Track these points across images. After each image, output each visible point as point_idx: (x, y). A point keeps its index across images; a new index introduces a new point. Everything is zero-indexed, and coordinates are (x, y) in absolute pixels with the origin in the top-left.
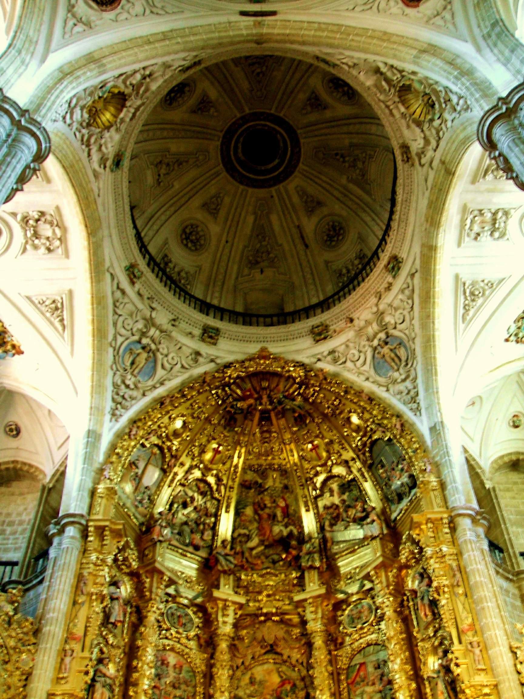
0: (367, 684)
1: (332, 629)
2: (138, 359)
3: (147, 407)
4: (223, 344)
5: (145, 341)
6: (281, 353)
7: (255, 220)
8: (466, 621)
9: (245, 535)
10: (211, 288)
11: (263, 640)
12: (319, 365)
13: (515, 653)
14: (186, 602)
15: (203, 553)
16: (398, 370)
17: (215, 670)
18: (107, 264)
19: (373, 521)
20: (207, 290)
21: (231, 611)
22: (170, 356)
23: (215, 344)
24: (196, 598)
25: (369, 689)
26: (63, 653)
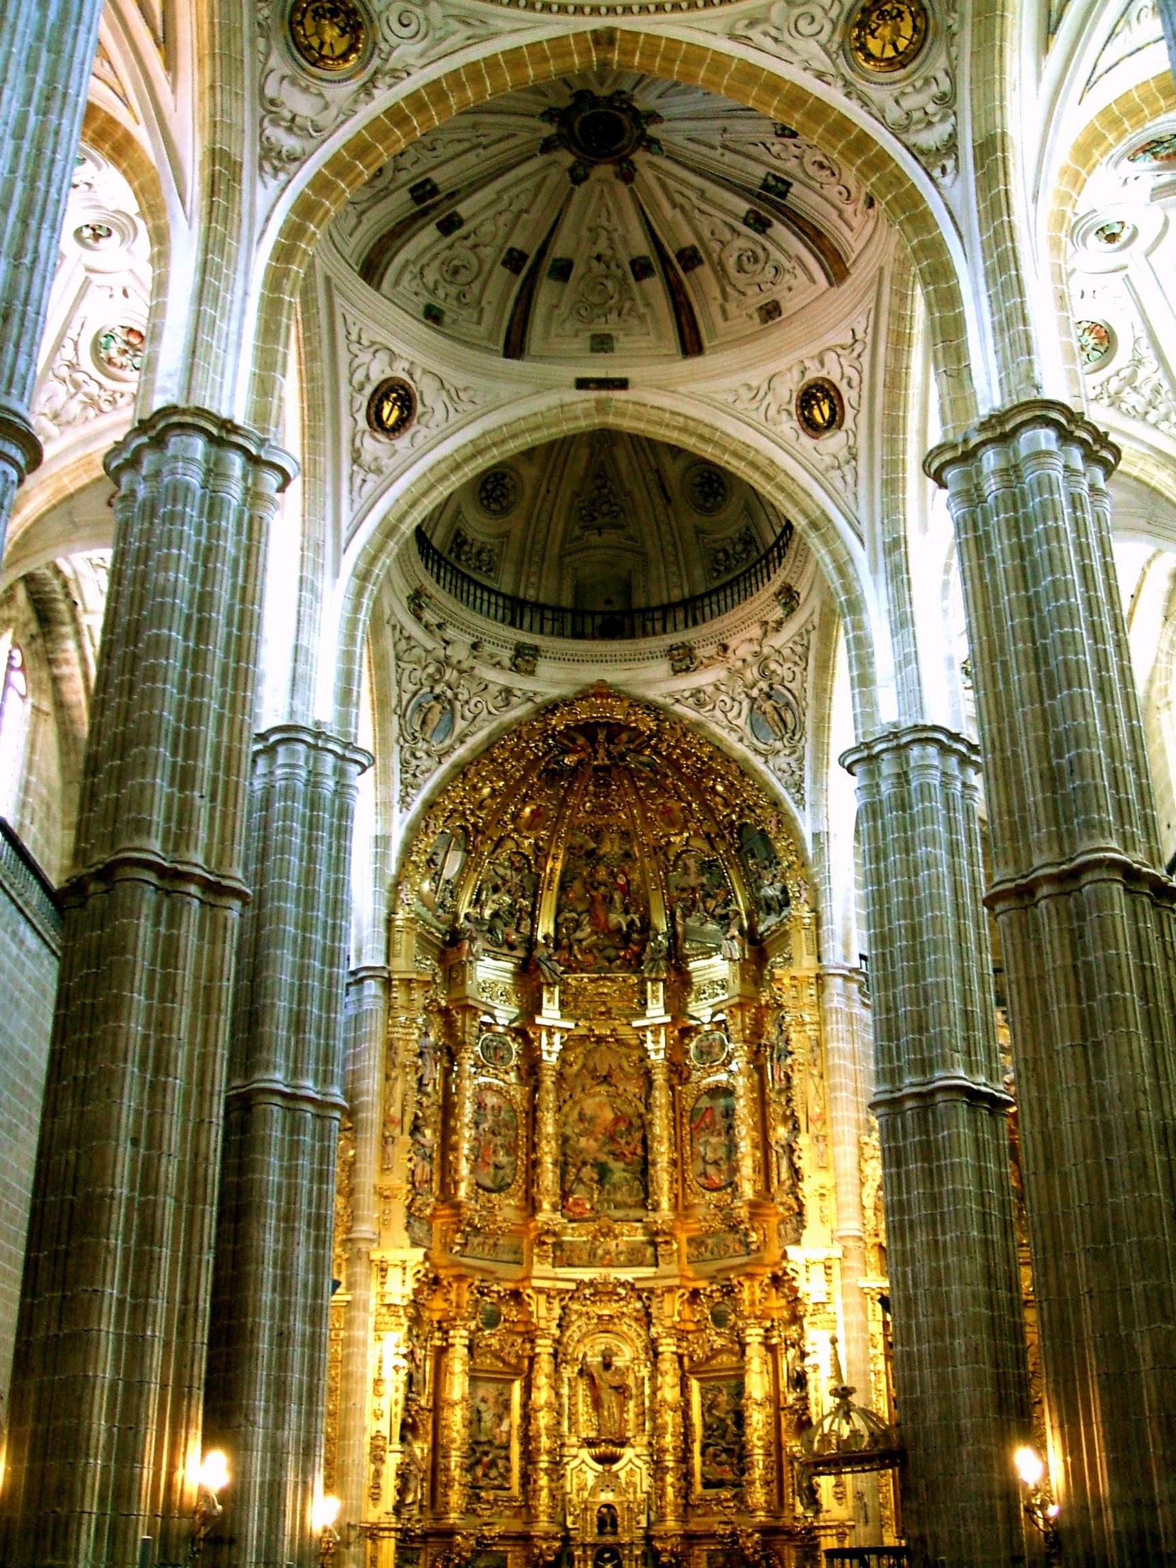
0: (712, 1133)
1: (678, 1058)
2: (430, 716)
3: (444, 778)
4: (545, 668)
5: (437, 690)
6: (626, 683)
7: (592, 455)
8: (815, 1110)
9: (573, 920)
10: (525, 566)
11: (595, 1069)
12: (678, 708)
13: (861, 1149)
14: (501, 1029)
15: (520, 953)
16: (782, 739)
17: (539, 1114)
18: (387, 612)
19: (733, 938)
20: (518, 574)
21: (557, 1038)
22: (473, 702)
23: (532, 673)
24: (512, 1021)
25: (714, 1140)
26: (386, 1141)
